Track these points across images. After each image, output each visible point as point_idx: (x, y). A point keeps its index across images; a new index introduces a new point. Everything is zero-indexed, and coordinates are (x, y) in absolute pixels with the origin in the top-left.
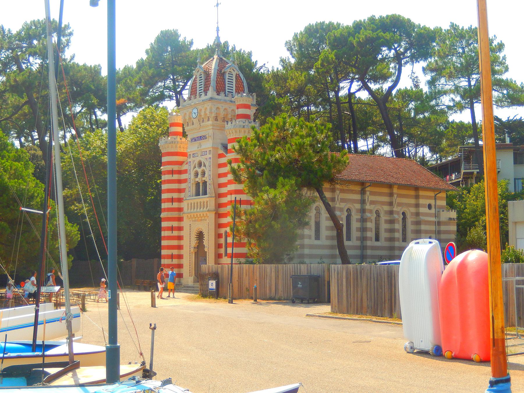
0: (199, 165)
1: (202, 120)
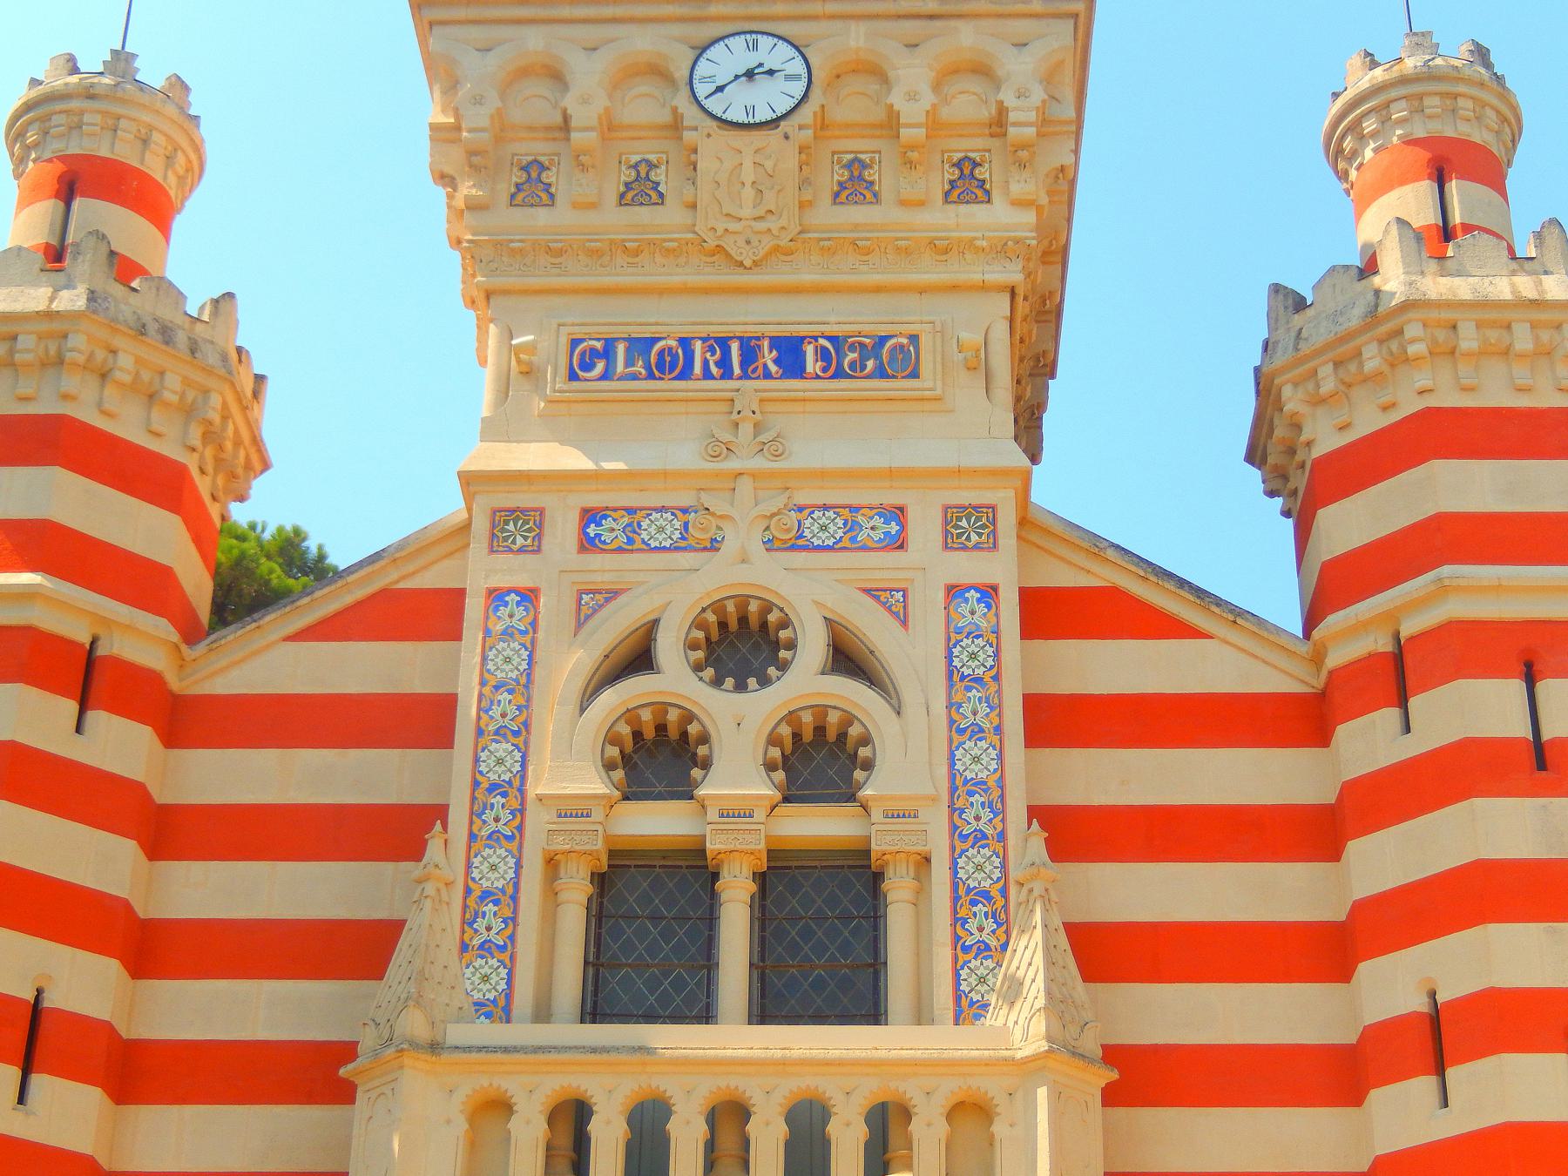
1: (829, 177)
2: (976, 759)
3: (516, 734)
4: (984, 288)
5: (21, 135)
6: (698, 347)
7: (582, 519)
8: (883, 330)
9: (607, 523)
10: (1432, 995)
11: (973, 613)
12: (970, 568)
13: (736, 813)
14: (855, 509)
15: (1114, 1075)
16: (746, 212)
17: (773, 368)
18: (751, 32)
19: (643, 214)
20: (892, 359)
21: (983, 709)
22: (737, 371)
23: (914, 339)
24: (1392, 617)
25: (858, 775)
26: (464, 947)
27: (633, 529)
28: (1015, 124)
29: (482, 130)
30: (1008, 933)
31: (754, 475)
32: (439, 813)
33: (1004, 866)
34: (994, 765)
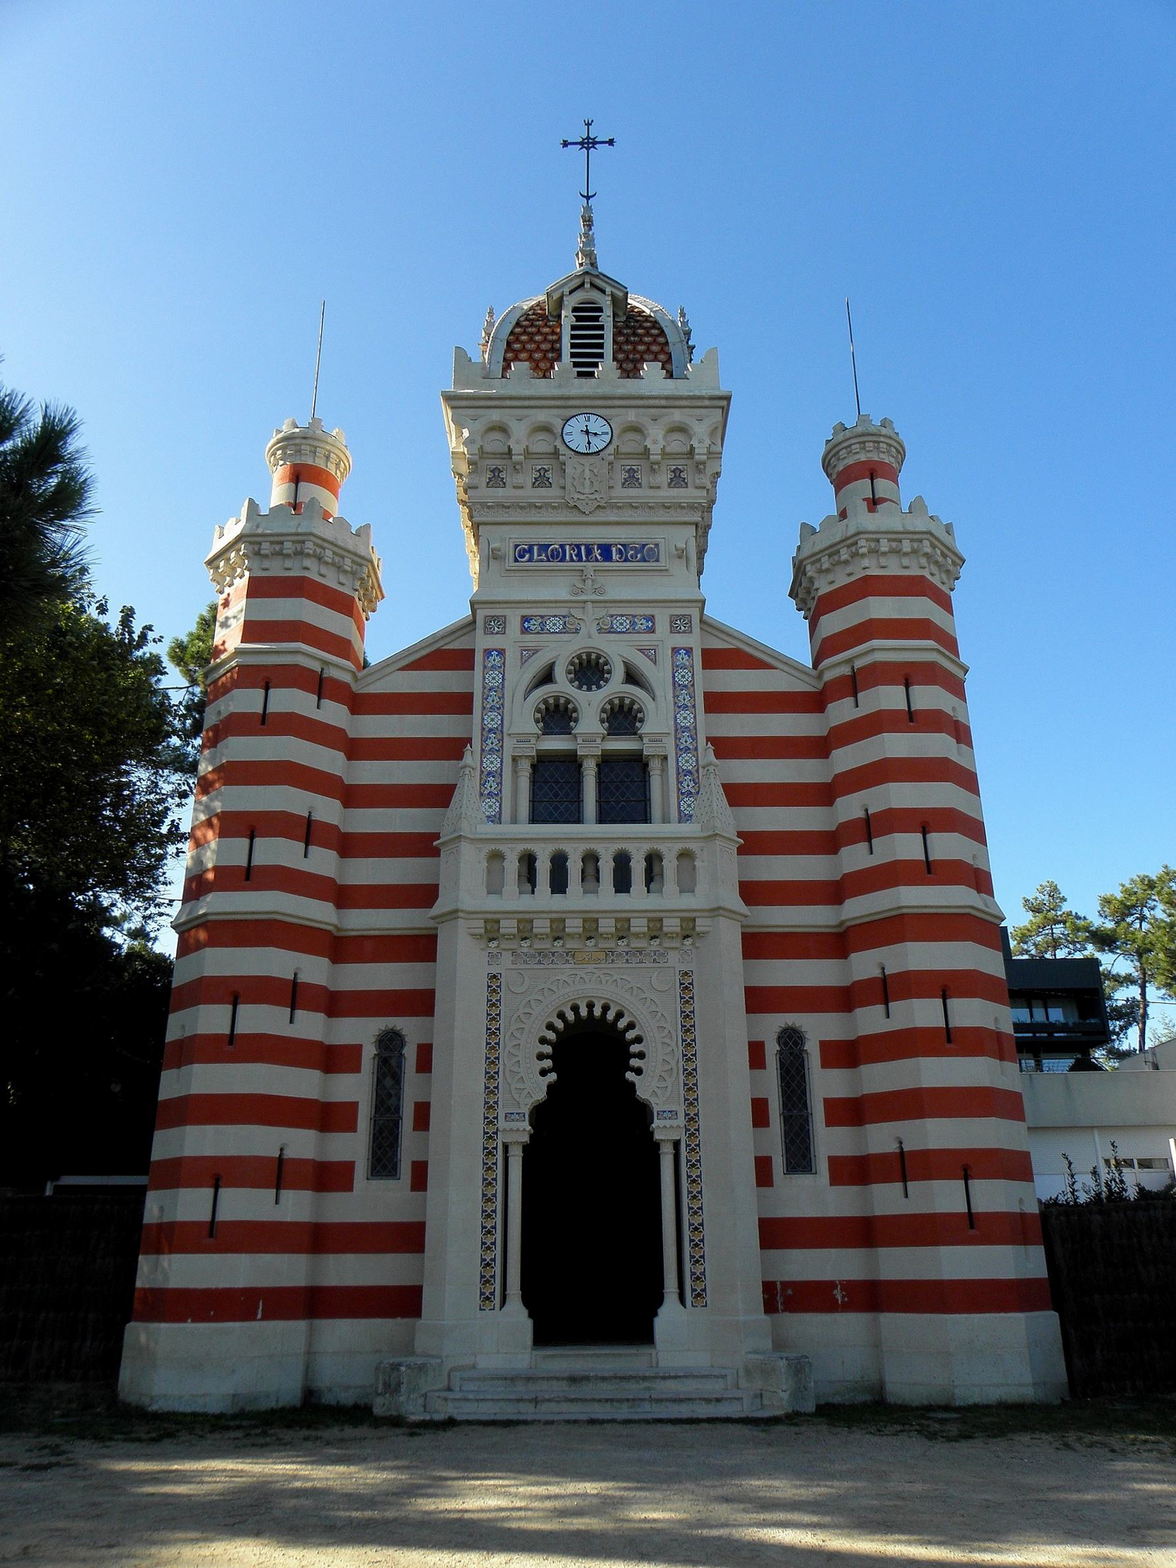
1: (620, 476)
2: (685, 718)
3: (499, 709)
5: (274, 454)
7: (522, 620)
8: (644, 541)
9: (533, 622)
10: (866, 810)
11: (683, 659)
12: (681, 640)
13: (589, 739)
14: (635, 616)
15: (742, 841)
16: (587, 491)
17: (599, 557)
18: (587, 414)
19: (543, 491)
20: (648, 554)
21: (688, 698)
22: (584, 558)
23: (657, 545)
24: (850, 661)
25: (638, 724)
26: (481, 794)
27: (543, 624)
28: (697, 454)
29: (475, 454)
30: (699, 787)
31: (592, 602)
32: (469, 740)
33: (697, 760)
34: (692, 721)
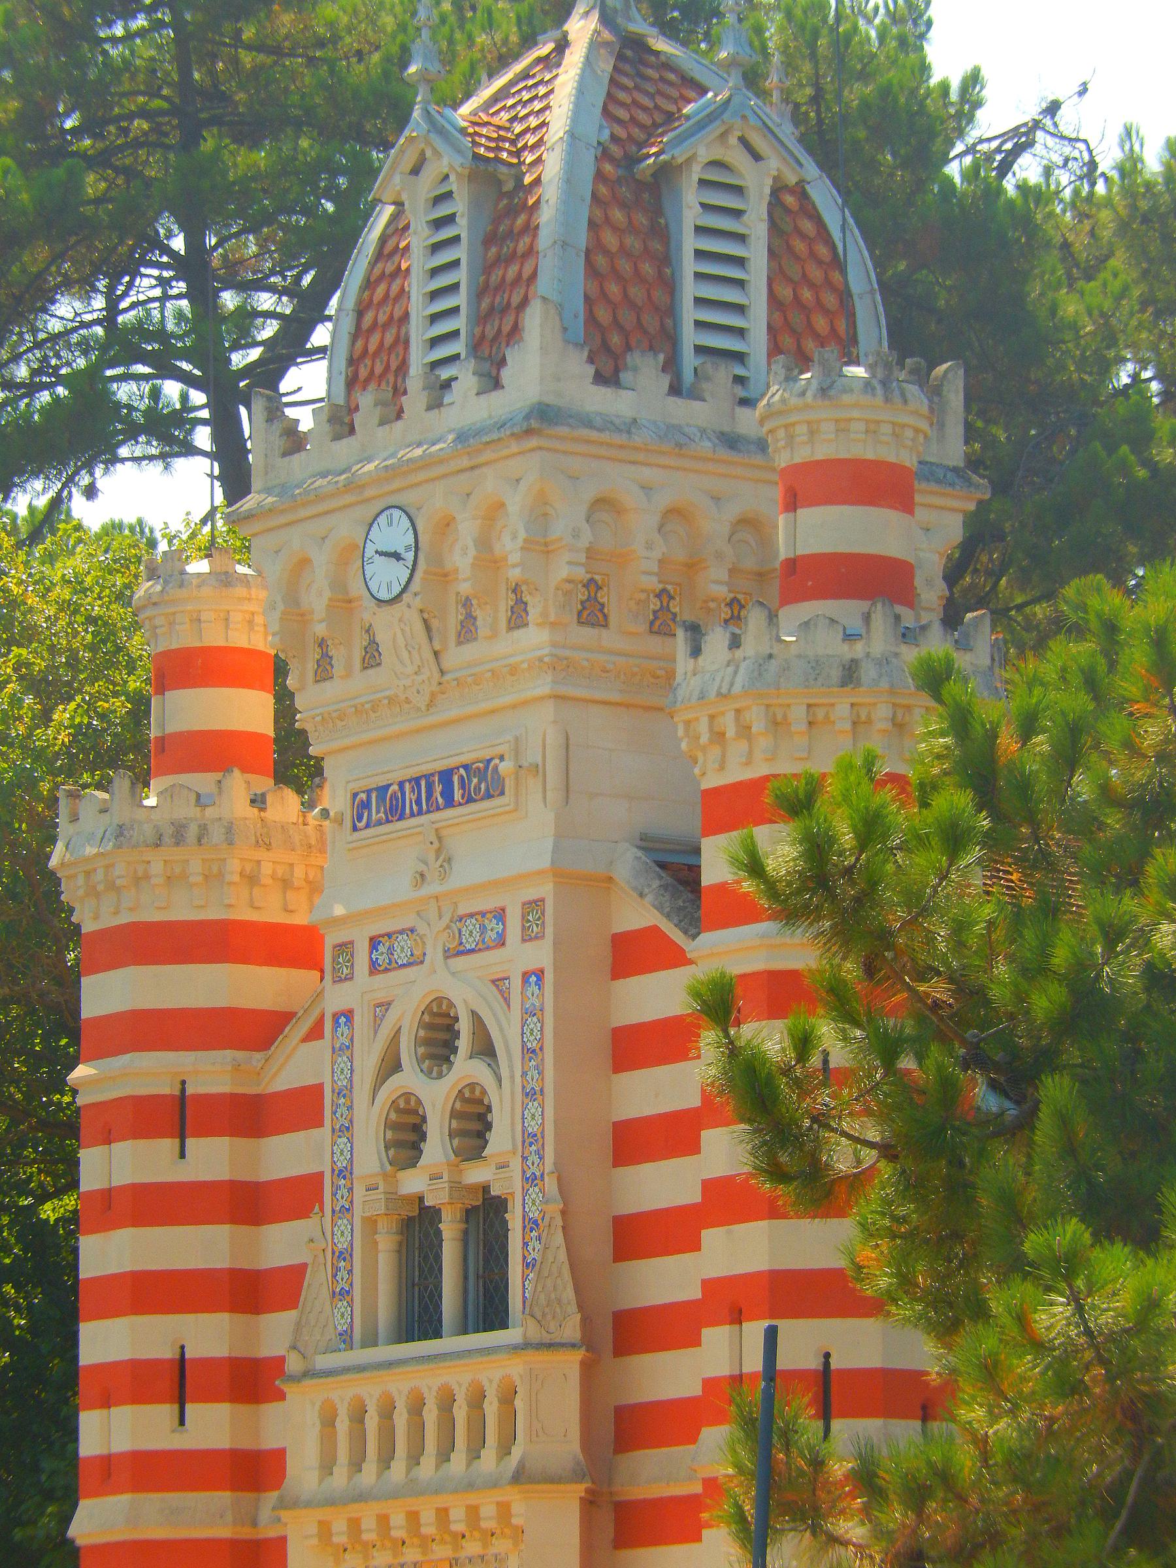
0: (427, 1042)
1: (454, 618)
4: (542, 698)
6: (407, 786)
9: (381, 948)
14: (483, 914)
16: (410, 669)
20: (492, 778)
27: (391, 950)
